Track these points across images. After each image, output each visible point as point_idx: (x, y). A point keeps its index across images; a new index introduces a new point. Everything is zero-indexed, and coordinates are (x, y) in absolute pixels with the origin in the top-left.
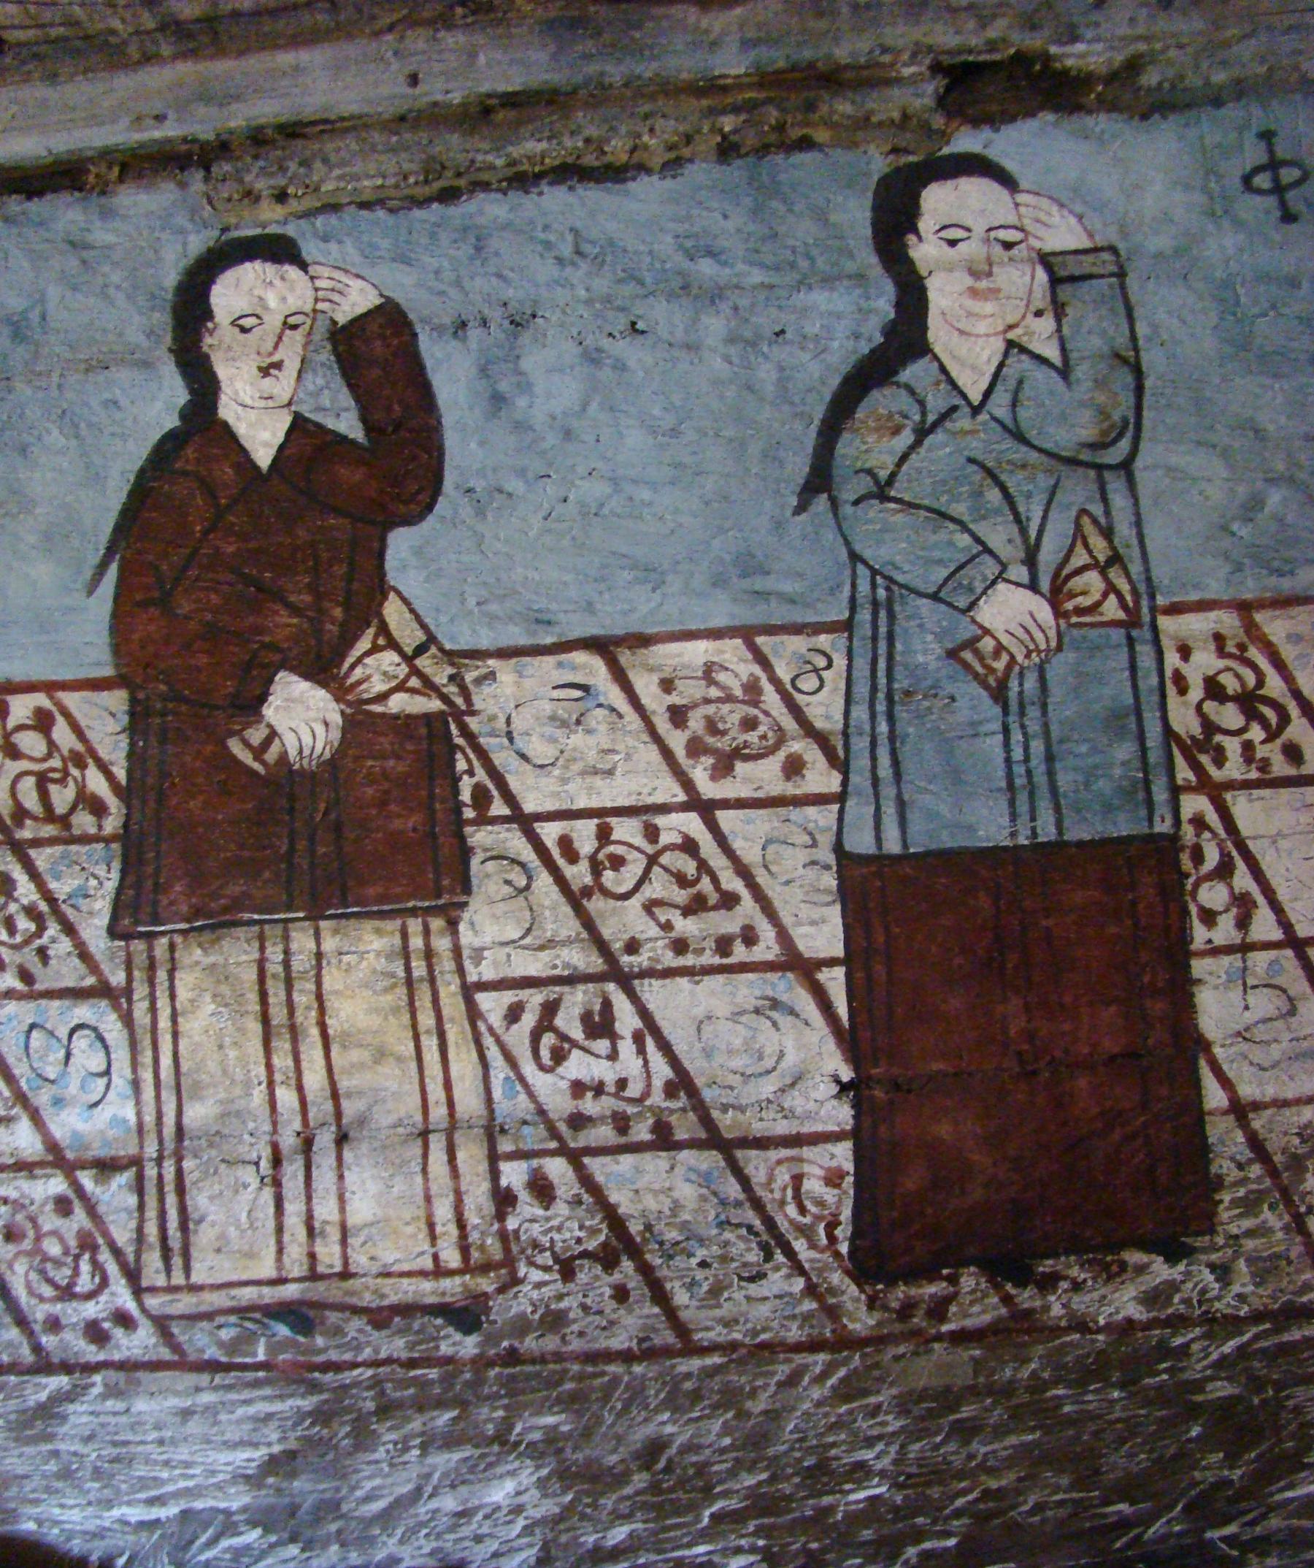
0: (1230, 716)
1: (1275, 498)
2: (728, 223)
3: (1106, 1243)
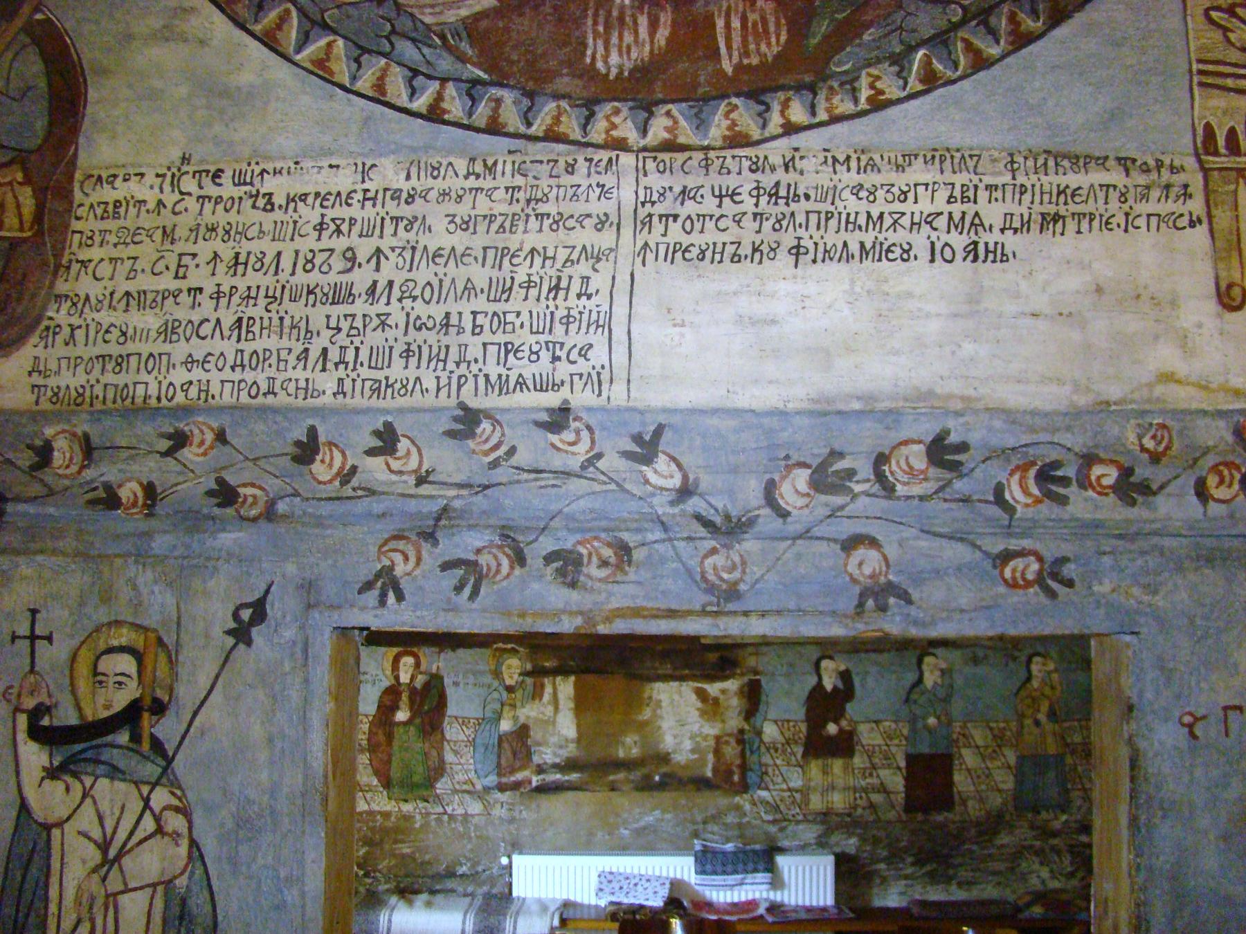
3: (939, 810)
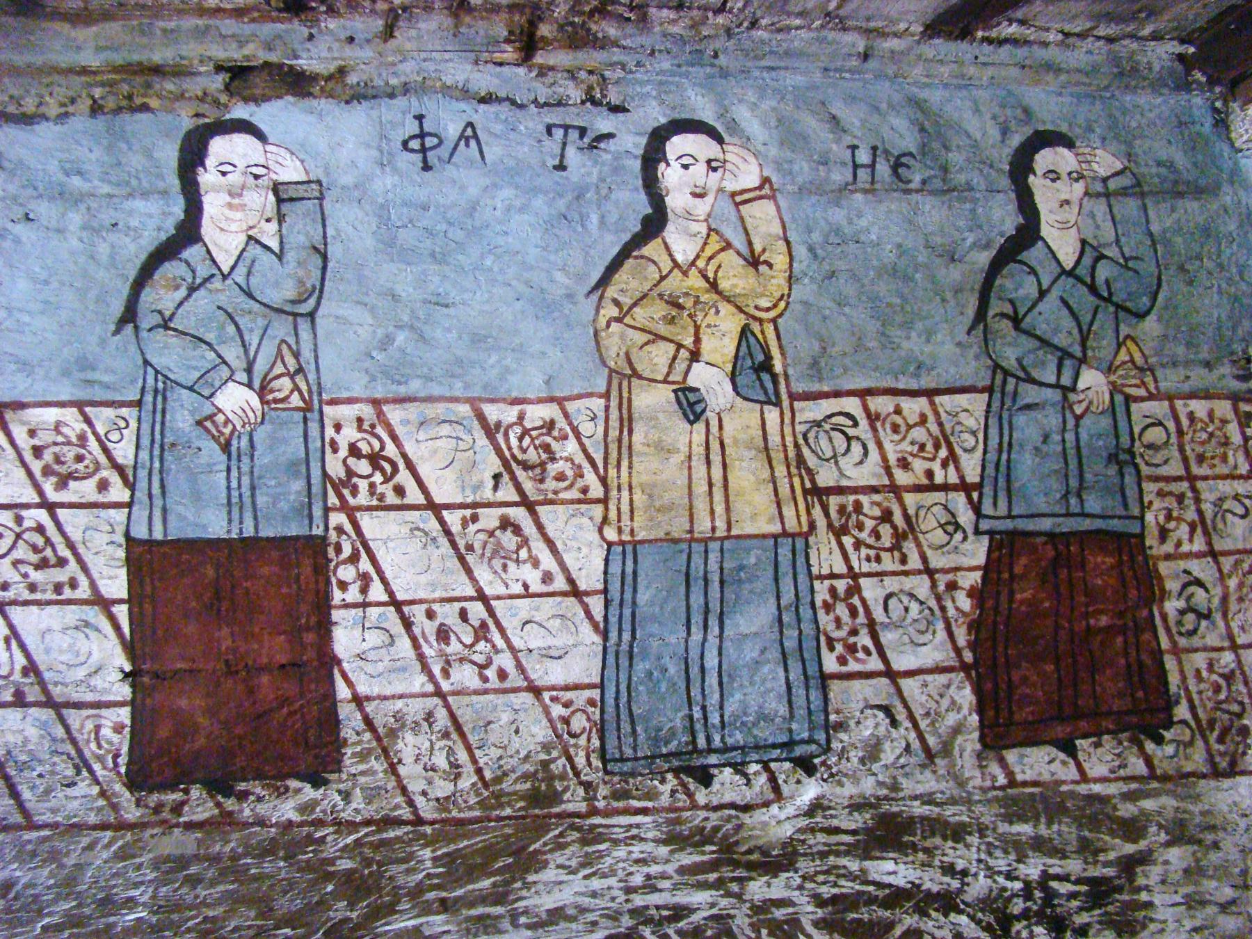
0: (363, 467)
1: (401, 337)
2: (92, 156)
3: (276, 775)
